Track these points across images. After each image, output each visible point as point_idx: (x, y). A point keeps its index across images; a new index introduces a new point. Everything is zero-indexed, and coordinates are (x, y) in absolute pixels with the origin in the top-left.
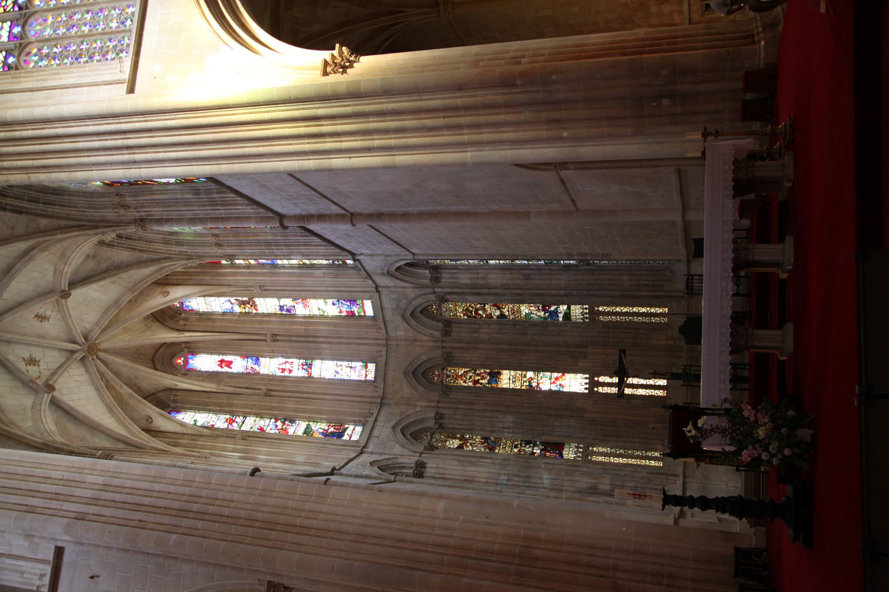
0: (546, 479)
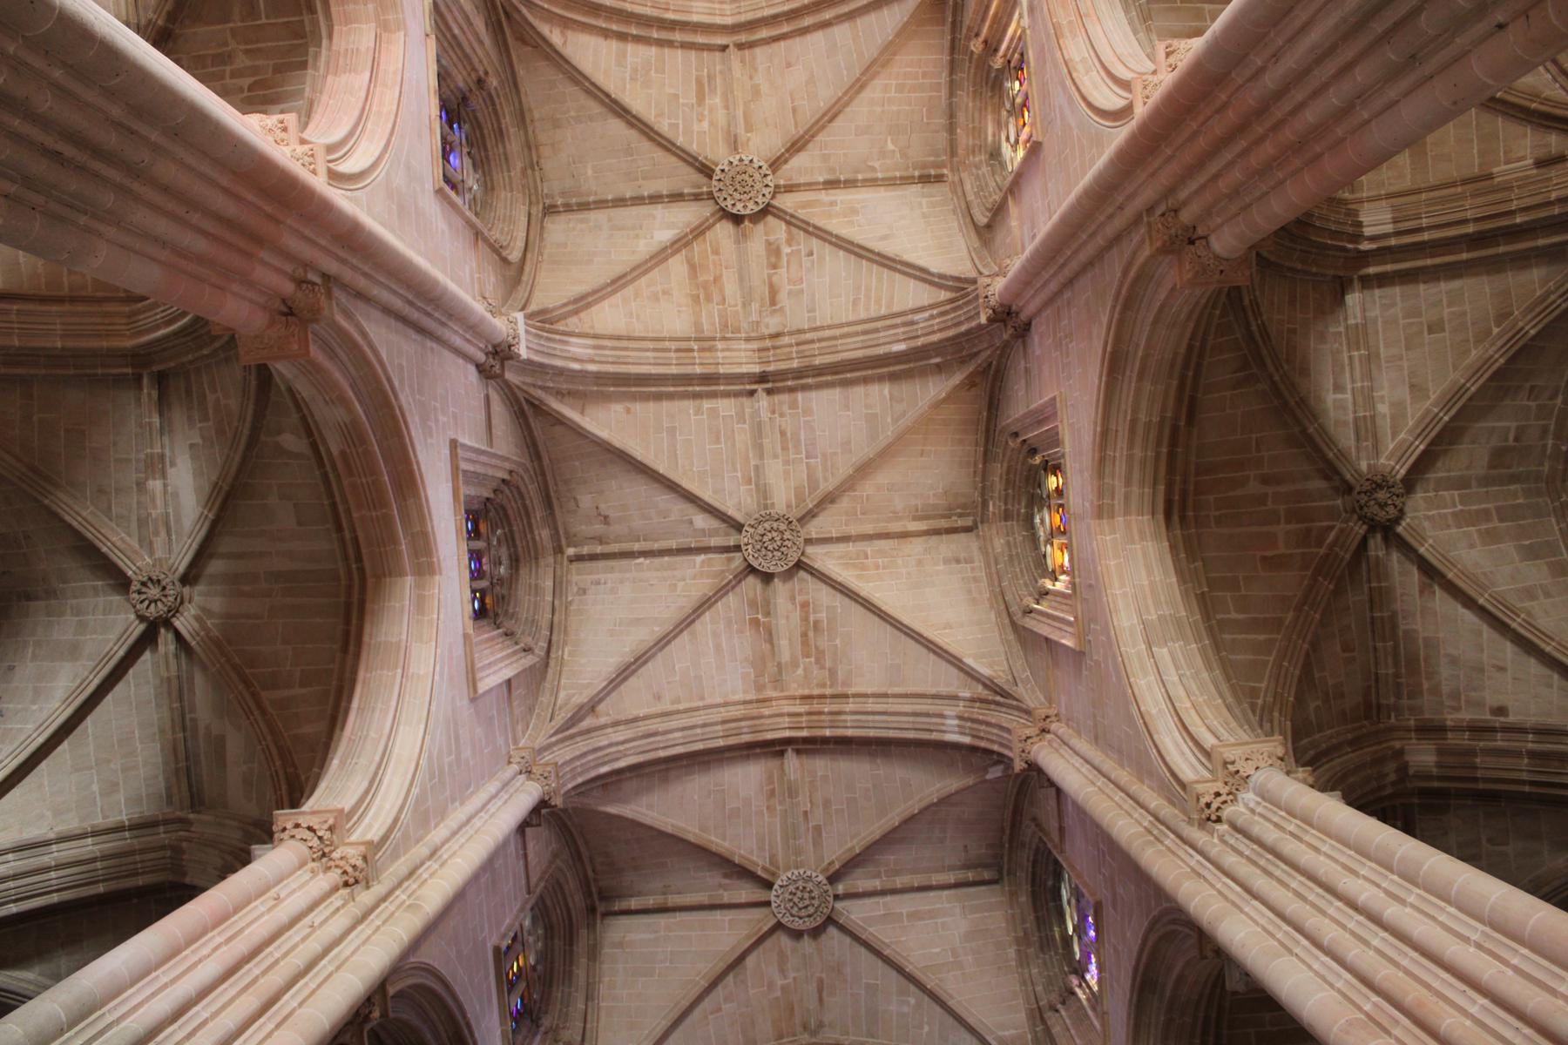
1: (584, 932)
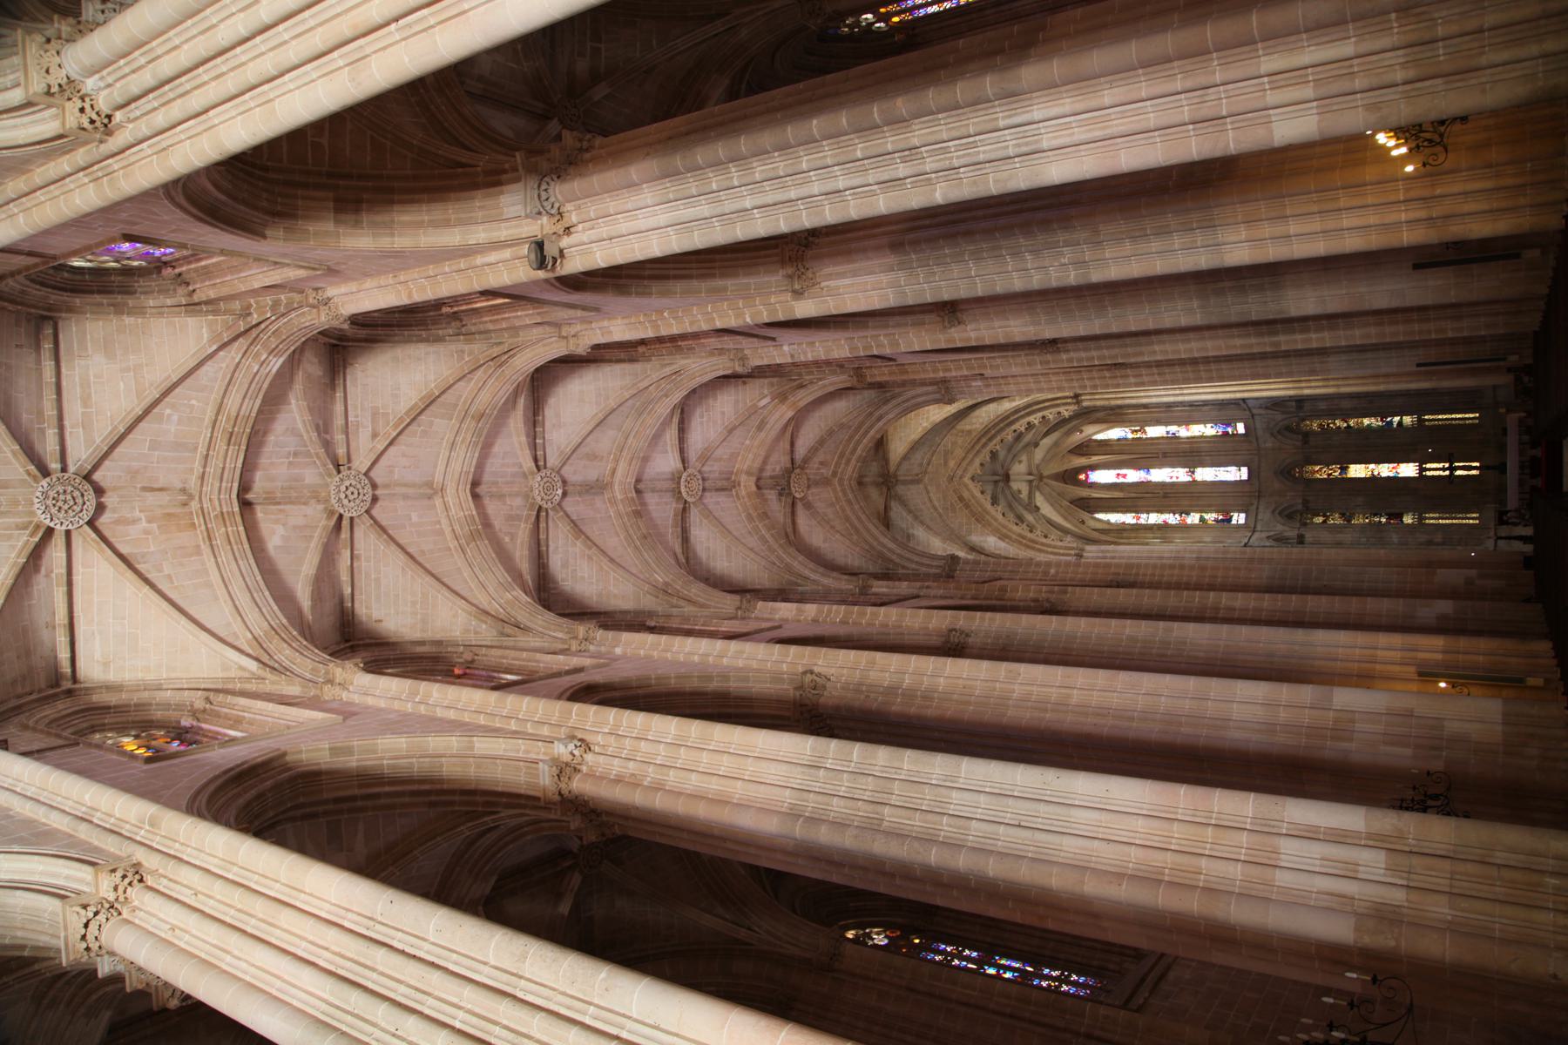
0: (1395, 538)
1: (95, 698)
